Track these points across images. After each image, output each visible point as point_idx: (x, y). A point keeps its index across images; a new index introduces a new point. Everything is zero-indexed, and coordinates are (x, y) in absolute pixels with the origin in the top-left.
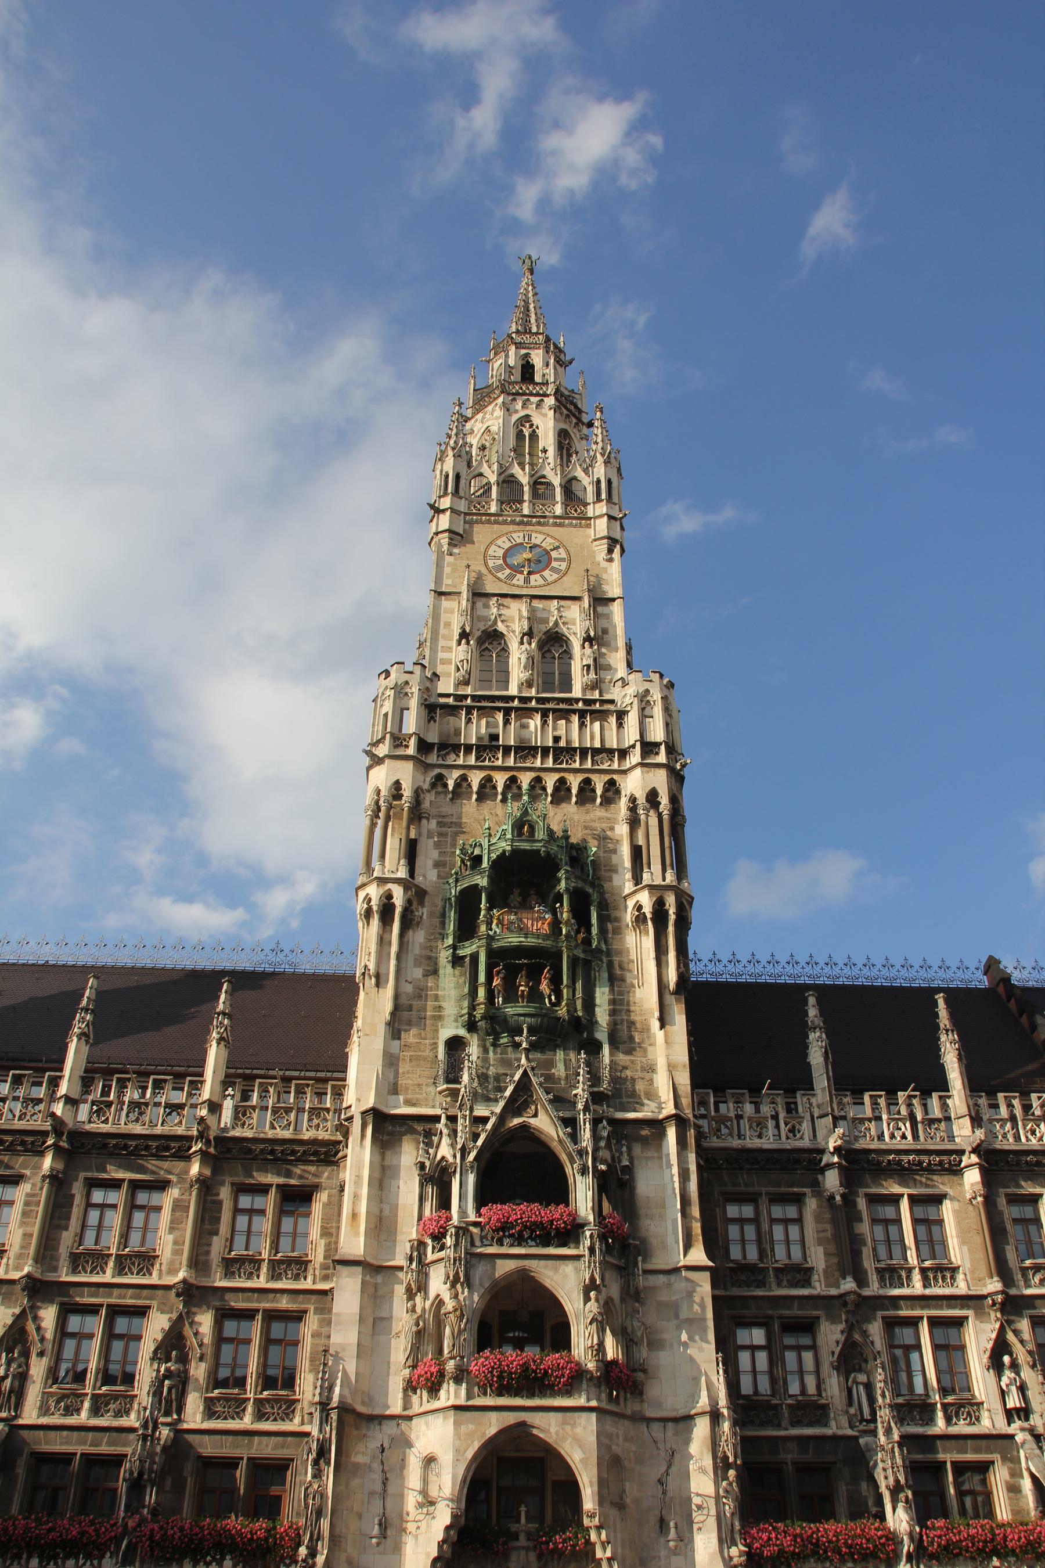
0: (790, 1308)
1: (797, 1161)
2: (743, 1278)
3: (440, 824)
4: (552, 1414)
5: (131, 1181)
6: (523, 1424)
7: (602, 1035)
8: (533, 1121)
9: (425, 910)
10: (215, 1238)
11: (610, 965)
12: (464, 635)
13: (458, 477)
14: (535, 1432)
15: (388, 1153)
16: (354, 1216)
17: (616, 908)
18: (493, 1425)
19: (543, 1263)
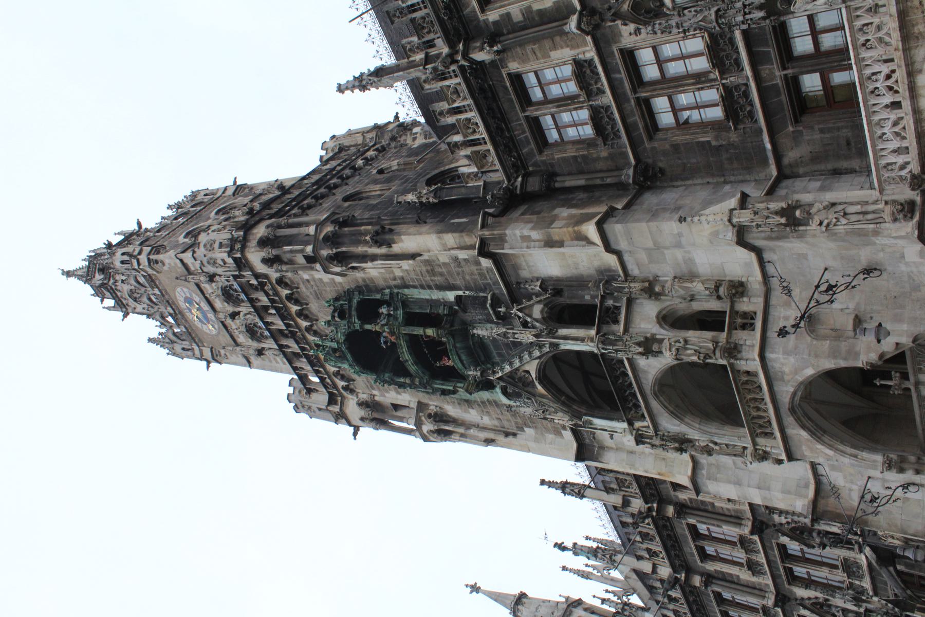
0: (621, 80)
1: (482, 90)
2: (609, 127)
3: (373, 389)
4: (776, 388)
5: (694, 541)
6: (792, 410)
7: (451, 296)
8: (534, 376)
9: (431, 403)
10: (716, 504)
11: (397, 287)
12: (260, 352)
13: (183, 349)
14: (797, 398)
15: (606, 444)
16: (659, 474)
17: (357, 281)
18: (798, 434)
19: (644, 381)
